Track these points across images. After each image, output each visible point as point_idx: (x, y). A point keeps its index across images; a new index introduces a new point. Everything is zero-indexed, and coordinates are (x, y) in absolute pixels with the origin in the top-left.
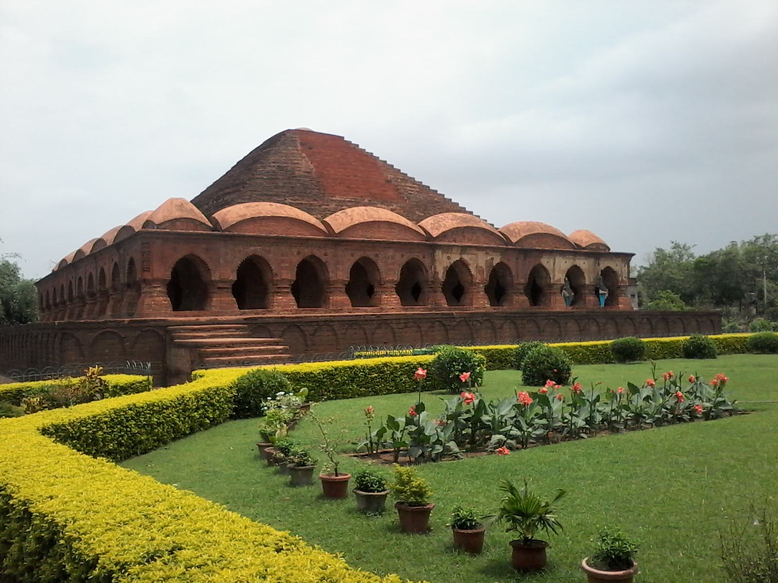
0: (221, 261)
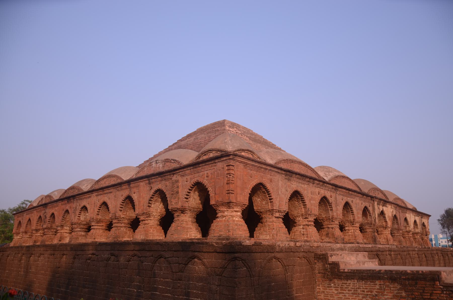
0: (280, 192)
